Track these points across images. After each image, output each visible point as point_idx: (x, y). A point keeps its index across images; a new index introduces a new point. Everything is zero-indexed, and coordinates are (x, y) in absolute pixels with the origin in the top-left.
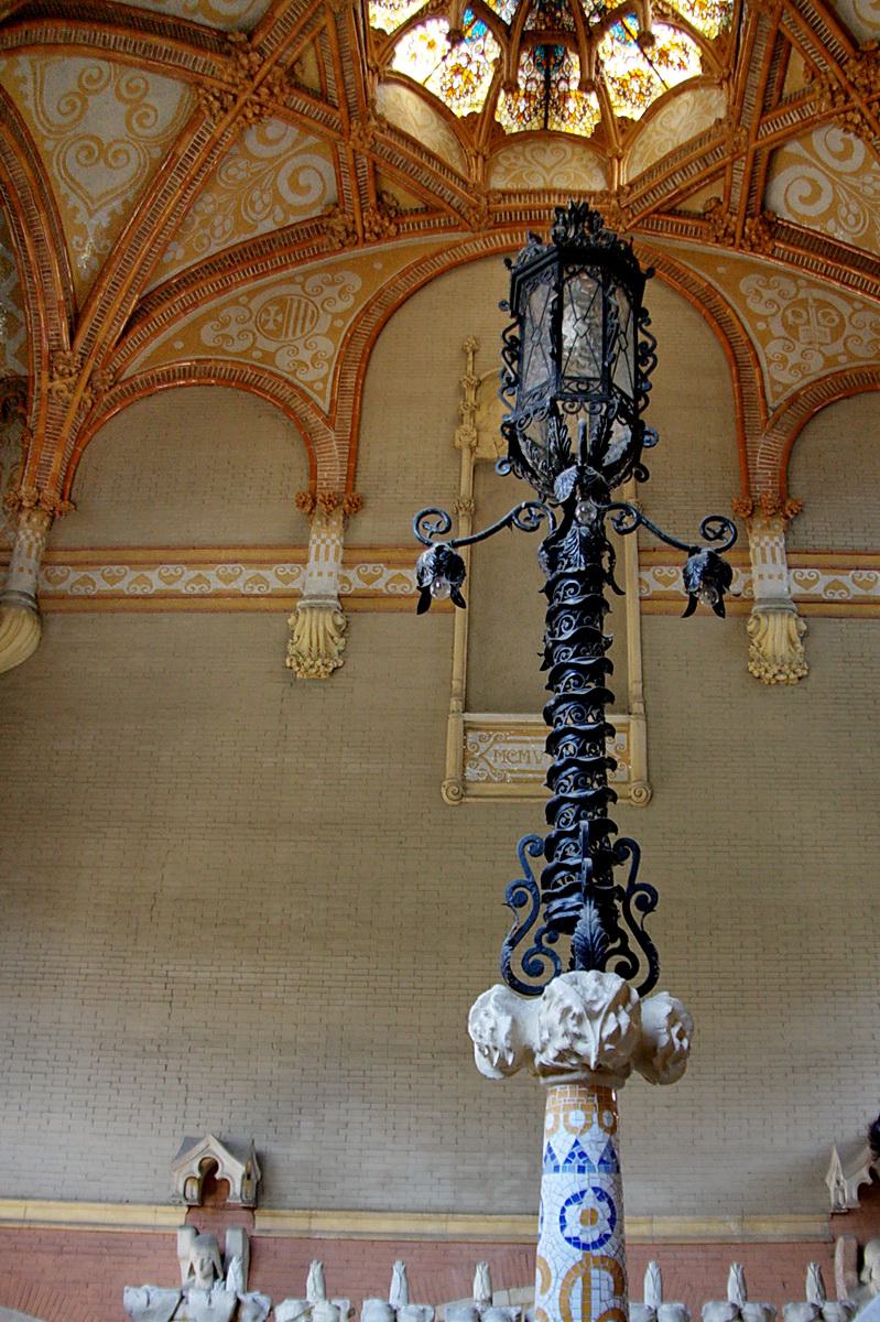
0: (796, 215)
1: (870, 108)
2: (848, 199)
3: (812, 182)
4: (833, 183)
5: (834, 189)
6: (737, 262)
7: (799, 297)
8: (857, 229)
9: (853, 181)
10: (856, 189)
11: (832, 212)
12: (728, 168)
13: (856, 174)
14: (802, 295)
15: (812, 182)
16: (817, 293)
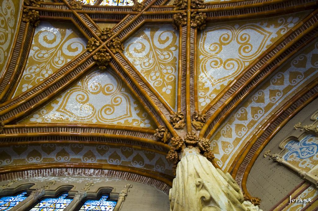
0: (38, 35)
1: (103, 48)
2: (50, 53)
3: (54, 40)
4: (56, 47)
5: (53, 48)
6: (19, 5)
7: (8, 27)
8: (37, 58)
9: (59, 53)
10: (56, 55)
11: (42, 48)
12: (62, 4)
13: (63, 54)
14: (9, 29)
15: (54, 40)
16: (10, 36)
